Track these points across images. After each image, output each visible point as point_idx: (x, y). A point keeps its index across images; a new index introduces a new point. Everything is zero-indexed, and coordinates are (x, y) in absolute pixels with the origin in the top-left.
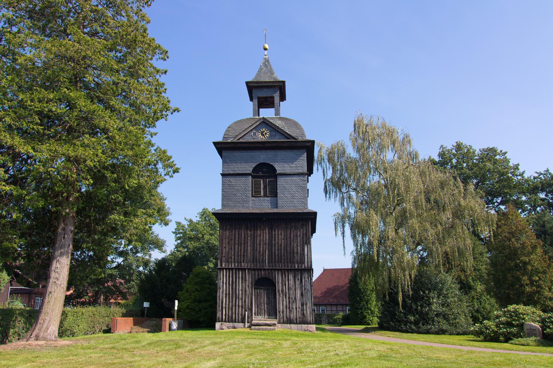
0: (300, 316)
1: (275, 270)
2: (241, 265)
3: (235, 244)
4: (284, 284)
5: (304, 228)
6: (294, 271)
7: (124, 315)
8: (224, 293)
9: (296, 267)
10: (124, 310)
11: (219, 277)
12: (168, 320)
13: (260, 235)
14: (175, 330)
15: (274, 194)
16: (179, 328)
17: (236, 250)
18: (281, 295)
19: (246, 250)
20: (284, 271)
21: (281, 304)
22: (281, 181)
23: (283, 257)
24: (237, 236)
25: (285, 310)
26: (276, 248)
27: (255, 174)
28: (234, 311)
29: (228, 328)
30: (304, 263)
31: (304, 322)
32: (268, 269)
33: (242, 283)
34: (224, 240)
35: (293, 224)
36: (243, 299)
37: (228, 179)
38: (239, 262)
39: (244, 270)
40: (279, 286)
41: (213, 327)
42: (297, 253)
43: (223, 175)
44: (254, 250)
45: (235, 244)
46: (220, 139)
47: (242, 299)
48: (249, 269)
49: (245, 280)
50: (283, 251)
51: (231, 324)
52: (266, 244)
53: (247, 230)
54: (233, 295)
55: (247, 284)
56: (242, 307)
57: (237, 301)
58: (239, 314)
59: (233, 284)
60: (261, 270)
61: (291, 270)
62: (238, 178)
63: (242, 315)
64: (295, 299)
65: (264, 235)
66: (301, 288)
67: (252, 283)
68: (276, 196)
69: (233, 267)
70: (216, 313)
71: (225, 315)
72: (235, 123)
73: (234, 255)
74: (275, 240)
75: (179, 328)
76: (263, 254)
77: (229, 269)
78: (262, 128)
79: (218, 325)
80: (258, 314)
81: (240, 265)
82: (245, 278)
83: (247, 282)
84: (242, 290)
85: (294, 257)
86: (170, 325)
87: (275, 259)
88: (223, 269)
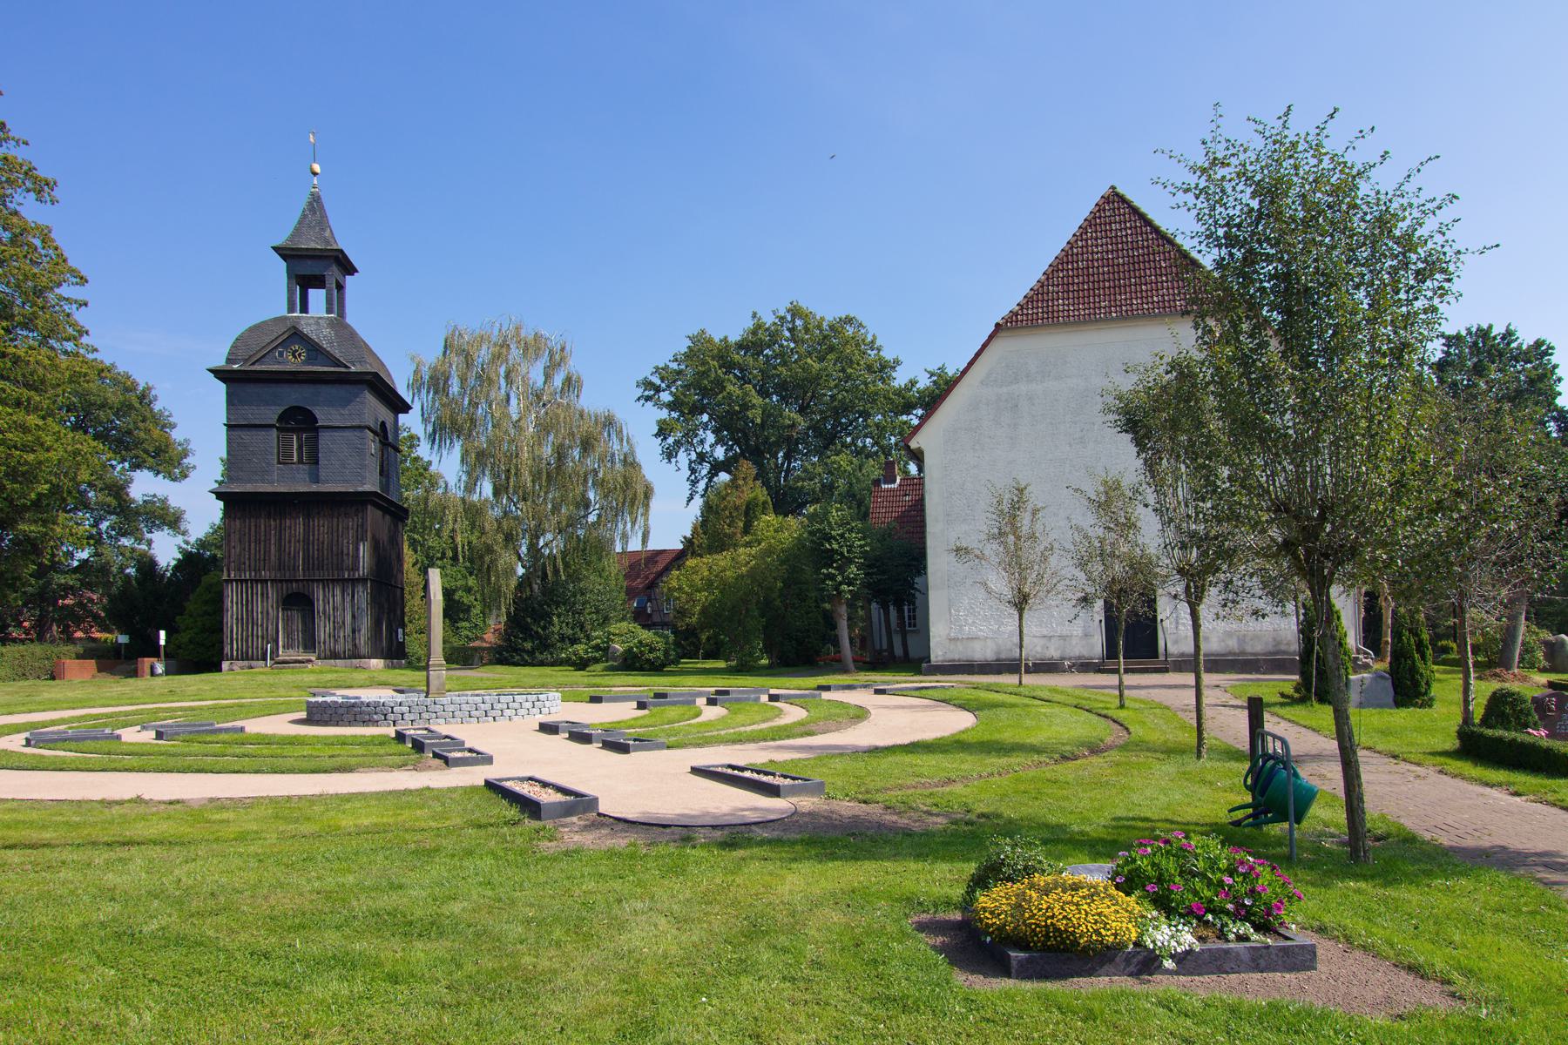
0: (350, 647)
1: (313, 581)
2: (260, 575)
3: (250, 542)
4: (326, 602)
5: (360, 515)
6: (343, 582)
7: (79, 657)
10: (79, 649)
11: (225, 594)
12: (148, 661)
13: (290, 528)
14: (161, 675)
15: (314, 460)
16: (167, 672)
17: (253, 551)
18: (323, 618)
20: (325, 582)
21: (323, 631)
22: (325, 439)
23: (325, 562)
24: (253, 528)
25: (327, 639)
27: (284, 425)
28: (250, 644)
29: (242, 668)
30: (358, 570)
31: (355, 655)
33: (262, 602)
34: (232, 536)
35: (342, 509)
37: (237, 433)
38: (257, 570)
40: (318, 605)
41: (220, 670)
42: (348, 554)
43: (230, 427)
44: (280, 549)
45: (250, 542)
46: (220, 362)
47: (262, 625)
48: (272, 581)
49: (267, 598)
50: (325, 552)
51: (246, 663)
52: (299, 541)
53: (269, 518)
54: (248, 620)
55: (270, 604)
56: (263, 638)
58: (257, 648)
59: (248, 604)
60: (291, 581)
61: (338, 581)
62: (254, 432)
63: (262, 649)
64: (344, 623)
65: (297, 526)
66: (353, 606)
67: (277, 602)
68: (317, 463)
69: (248, 577)
70: (223, 649)
71: (237, 650)
72: (251, 330)
73: (249, 559)
74: (314, 535)
75: (167, 672)
76: (295, 557)
77: (242, 581)
78: (293, 344)
79: (225, 665)
80: (287, 646)
82: (267, 594)
83: (270, 600)
84: (262, 613)
85: (343, 561)
86: (152, 668)
87: (313, 564)
88: (232, 581)
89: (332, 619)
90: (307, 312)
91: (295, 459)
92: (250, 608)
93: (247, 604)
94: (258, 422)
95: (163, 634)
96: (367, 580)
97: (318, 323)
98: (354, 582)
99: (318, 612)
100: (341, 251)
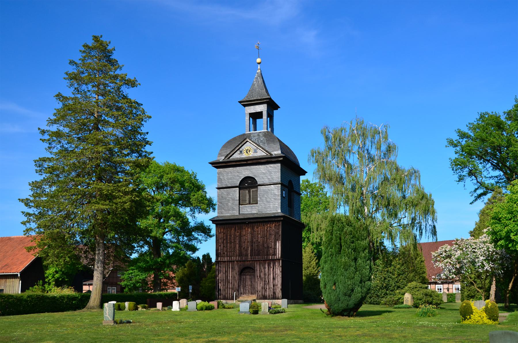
9: (270, 258)
19: (235, 247)
26: (256, 245)
28: (226, 292)
32: (250, 261)
35: (269, 225)
36: (233, 283)
44: (240, 247)
47: (232, 283)
57: (229, 284)
58: (230, 294)
63: (232, 294)
69: (226, 260)
81: (230, 259)
84: (232, 277)
91: (247, 202)
92: (226, 275)
93: (225, 273)
94: (230, 185)
95: (190, 287)
96: (280, 260)
97: (259, 135)
98: (274, 261)
99: (257, 276)
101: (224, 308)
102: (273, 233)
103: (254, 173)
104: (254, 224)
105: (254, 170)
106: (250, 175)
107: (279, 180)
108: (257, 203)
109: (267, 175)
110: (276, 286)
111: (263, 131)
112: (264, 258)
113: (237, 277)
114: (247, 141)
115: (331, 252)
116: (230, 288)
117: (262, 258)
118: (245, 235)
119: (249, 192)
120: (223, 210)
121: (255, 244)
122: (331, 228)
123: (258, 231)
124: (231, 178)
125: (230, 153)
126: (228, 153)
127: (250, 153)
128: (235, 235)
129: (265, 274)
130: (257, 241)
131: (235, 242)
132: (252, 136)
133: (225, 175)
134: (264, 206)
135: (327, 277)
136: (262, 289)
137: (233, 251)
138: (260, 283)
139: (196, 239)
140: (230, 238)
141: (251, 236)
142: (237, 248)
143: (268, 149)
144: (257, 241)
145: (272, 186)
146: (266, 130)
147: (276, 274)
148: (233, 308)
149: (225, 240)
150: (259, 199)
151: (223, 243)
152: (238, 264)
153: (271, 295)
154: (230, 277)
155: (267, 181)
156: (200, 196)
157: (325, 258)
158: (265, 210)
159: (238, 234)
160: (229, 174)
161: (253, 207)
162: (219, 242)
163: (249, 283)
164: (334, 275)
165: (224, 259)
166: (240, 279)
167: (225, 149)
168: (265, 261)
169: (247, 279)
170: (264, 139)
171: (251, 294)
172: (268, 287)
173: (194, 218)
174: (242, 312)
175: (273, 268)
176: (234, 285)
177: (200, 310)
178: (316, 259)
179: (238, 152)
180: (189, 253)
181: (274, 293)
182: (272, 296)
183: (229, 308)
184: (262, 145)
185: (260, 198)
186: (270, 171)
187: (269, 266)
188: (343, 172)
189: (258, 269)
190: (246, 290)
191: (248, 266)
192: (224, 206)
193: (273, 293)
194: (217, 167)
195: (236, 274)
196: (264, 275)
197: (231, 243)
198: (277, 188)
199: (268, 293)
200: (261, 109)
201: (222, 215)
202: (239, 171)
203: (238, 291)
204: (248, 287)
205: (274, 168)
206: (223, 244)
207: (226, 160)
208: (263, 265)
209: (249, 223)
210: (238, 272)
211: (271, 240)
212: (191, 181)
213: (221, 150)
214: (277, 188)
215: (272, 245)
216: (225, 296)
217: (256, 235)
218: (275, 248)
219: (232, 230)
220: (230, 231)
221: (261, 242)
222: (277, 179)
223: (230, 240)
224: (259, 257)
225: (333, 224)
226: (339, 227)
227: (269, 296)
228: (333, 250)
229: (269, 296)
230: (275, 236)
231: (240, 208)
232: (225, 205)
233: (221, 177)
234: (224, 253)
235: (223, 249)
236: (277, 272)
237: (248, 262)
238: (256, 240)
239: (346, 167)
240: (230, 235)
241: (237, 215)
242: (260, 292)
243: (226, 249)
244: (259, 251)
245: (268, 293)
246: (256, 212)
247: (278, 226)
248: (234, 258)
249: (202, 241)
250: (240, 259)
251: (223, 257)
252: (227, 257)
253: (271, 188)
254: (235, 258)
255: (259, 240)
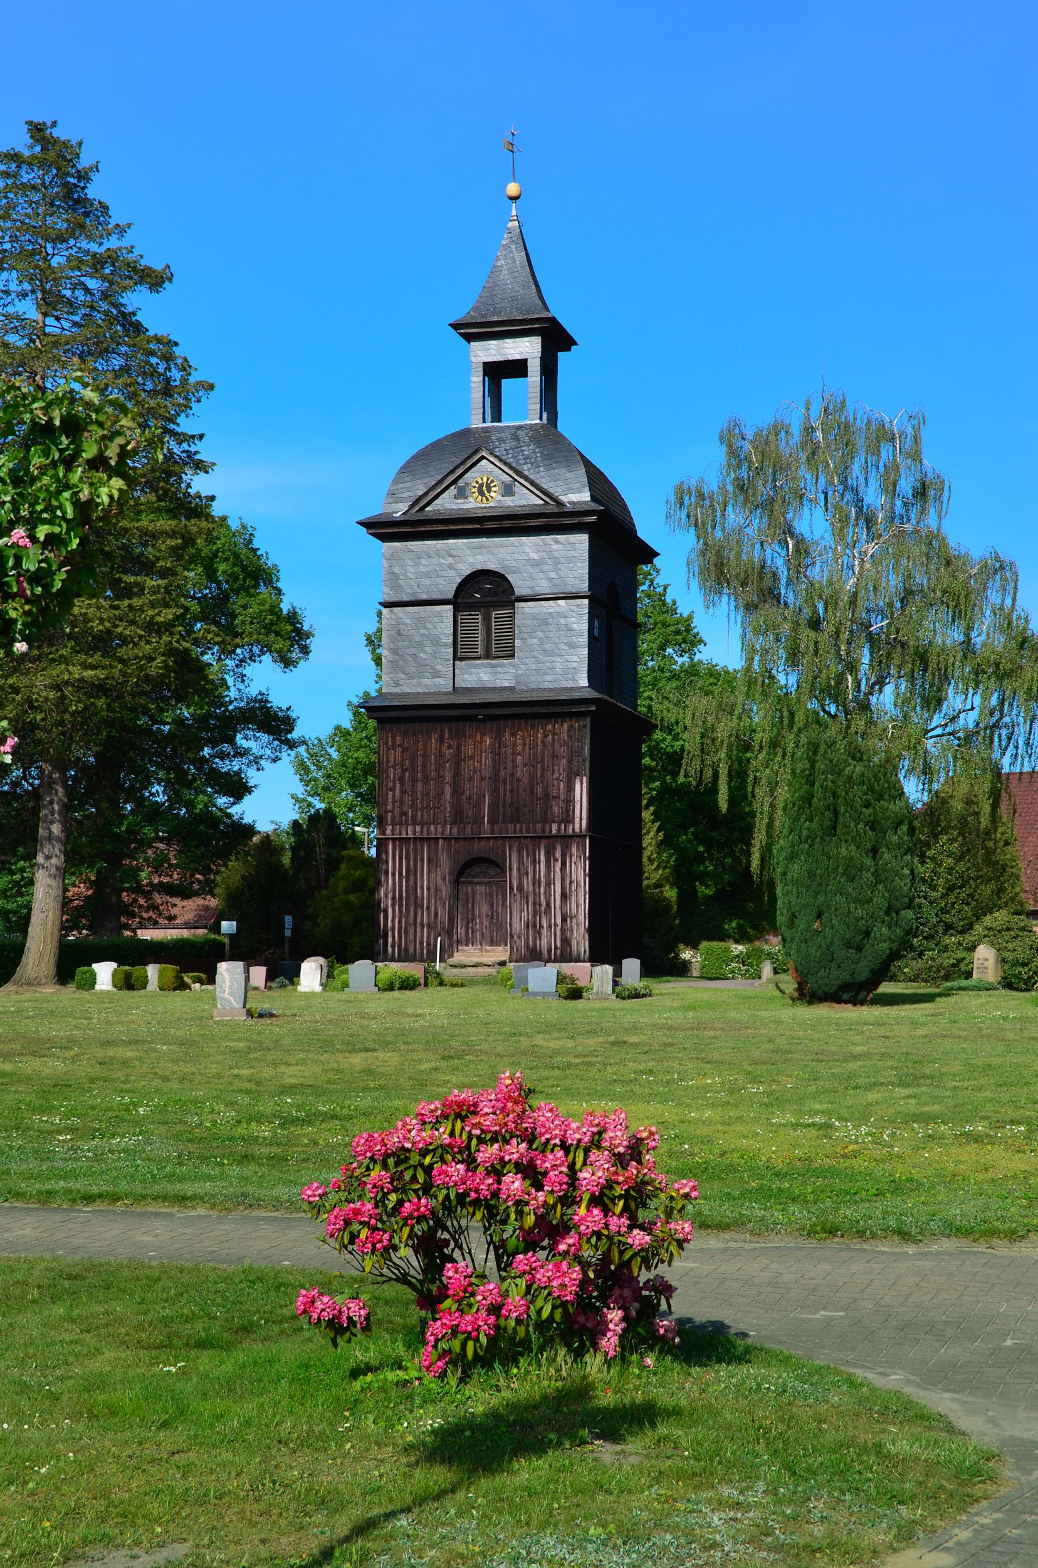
2: (429, 832)
4: (523, 873)
8: (390, 896)
9: (554, 832)
19: (440, 794)
26: (508, 787)
28: (411, 937)
30: (572, 821)
35: (549, 727)
36: (433, 909)
39: (432, 841)
44: (457, 792)
47: (428, 908)
54: (411, 901)
58: (421, 943)
63: (428, 944)
69: (410, 836)
84: (428, 889)
89: (531, 899)
90: (500, 421)
91: (480, 651)
92: (411, 883)
93: (407, 876)
95: (288, 920)
96: (585, 836)
98: (566, 839)
99: (511, 888)
100: (553, 320)
101: (441, 984)
102: (563, 750)
103: (503, 560)
104: (502, 723)
105: (503, 550)
106: (492, 566)
107: (584, 586)
108: (513, 656)
109: (546, 567)
110: (571, 918)
111: (528, 422)
112: (535, 832)
113: (445, 890)
114: (483, 458)
115: (808, 829)
116: (422, 926)
117: (528, 831)
118: (472, 757)
119: (487, 619)
120: (402, 676)
121: (505, 784)
122: (808, 766)
123: (515, 745)
124: (427, 575)
125: (426, 494)
126: (421, 493)
127: (493, 494)
128: (441, 756)
129: (536, 882)
130: (512, 775)
131: (440, 777)
132: (494, 438)
133: (410, 562)
134: (534, 667)
135: (798, 897)
136: (528, 927)
137: (434, 807)
138: (521, 911)
139: (246, 752)
140: (424, 766)
141: (493, 760)
142: (448, 797)
143: (551, 484)
144: (512, 775)
145: (562, 602)
146: (538, 421)
147: (571, 883)
148: (462, 985)
149: (406, 770)
150: (518, 643)
151: (402, 779)
152: (450, 847)
153: (556, 947)
154: (422, 888)
155: (543, 586)
156: (267, 606)
157: (793, 846)
158: (539, 678)
159: (449, 753)
160: (424, 561)
161: (499, 669)
162: (387, 777)
163: (485, 909)
164: (817, 893)
165: (404, 832)
166: (455, 897)
167: (408, 479)
168: (536, 839)
169: (478, 897)
170: (534, 452)
171: (492, 944)
172: (545, 924)
173: (243, 681)
174: (536, 994)
175: (564, 864)
176: (436, 915)
177: (386, 990)
178: (658, 831)
179: (453, 490)
180: (222, 801)
181: (566, 941)
182: (559, 952)
183: (453, 985)
184: (529, 470)
185: (523, 639)
186: (555, 554)
187: (549, 855)
188: (780, 562)
189: (515, 866)
190: (473, 931)
191: (483, 855)
192: (406, 660)
193: (562, 940)
194: (384, 538)
195: (444, 879)
196: (534, 884)
197: (426, 779)
198: (575, 609)
199: (544, 941)
200: (522, 350)
201: (397, 690)
202: (454, 552)
203: (449, 933)
204: (481, 923)
205: (569, 547)
206: (402, 785)
207: (414, 516)
208: (531, 852)
209: (487, 718)
210: (451, 873)
211: (557, 775)
212: (236, 555)
213: (395, 481)
214: (575, 609)
215: (558, 789)
216: (407, 950)
217: (510, 758)
218: (569, 800)
219: (430, 738)
220: (425, 745)
221: (526, 780)
222: (578, 582)
223: (423, 772)
224: (518, 826)
225: (815, 753)
226: (831, 761)
227: (549, 951)
228: (814, 825)
229: (549, 951)
230: (570, 762)
231: (457, 671)
232: (409, 658)
233: (396, 570)
234: (405, 814)
235: (401, 799)
236: (574, 876)
237: (483, 843)
238: (509, 772)
239: (791, 546)
240: (426, 757)
241: (446, 694)
242: (519, 937)
243: (413, 801)
244: (518, 809)
245: (544, 941)
246: (506, 684)
247: (579, 730)
248: (436, 829)
249: (262, 762)
250: (455, 831)
251: (401, 824)
252: (414, 824)
253: (558, 609)
254: (440, 830)
255: (519, 774)
